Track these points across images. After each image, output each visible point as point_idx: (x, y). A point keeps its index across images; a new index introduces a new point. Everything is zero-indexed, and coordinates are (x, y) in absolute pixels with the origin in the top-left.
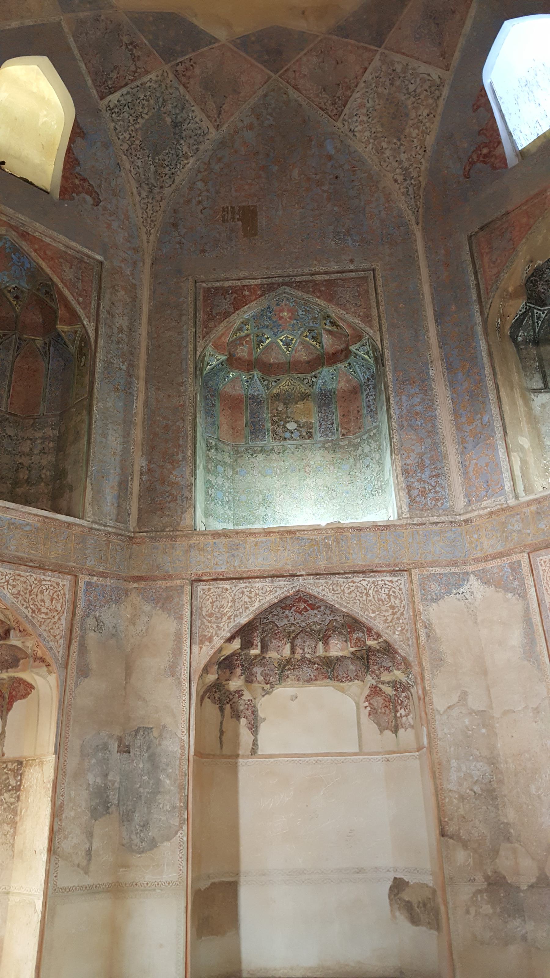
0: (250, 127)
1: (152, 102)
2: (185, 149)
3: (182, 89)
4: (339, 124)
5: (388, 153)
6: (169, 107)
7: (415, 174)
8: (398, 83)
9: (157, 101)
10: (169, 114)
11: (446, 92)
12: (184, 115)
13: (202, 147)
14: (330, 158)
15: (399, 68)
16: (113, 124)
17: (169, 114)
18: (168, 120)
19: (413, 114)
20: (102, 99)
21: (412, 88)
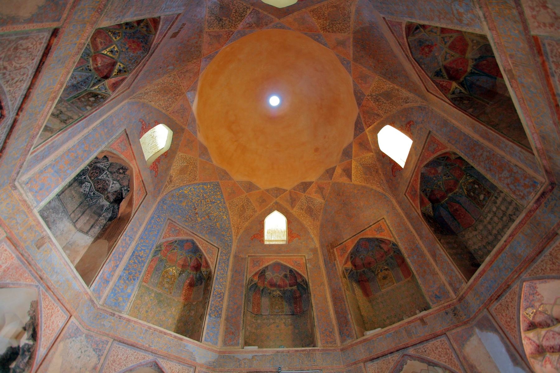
0: (197, 43)
1: (234, 19)
2: (212, 18)
3: (227, 30)
4: (175, 73)
5: (156, 87)
6: (227, 22)
7: (145, 97)
8: (174, 96)
9: (232, 19)
10: (225, 20)
11: (164, 111)
12: (220, 25)
13: (207, 24)
14: (168, 66)
15: (177, 97)
16: (244, 4)
17: (225, 20)
18: (224, 19)
19: (163, 99)
20: (253, 9)
21: (170, 100)
